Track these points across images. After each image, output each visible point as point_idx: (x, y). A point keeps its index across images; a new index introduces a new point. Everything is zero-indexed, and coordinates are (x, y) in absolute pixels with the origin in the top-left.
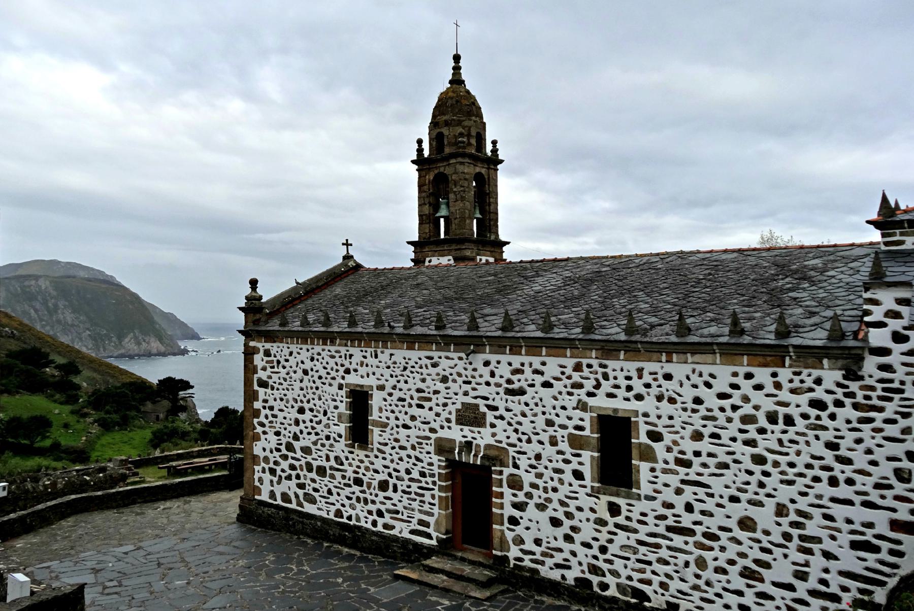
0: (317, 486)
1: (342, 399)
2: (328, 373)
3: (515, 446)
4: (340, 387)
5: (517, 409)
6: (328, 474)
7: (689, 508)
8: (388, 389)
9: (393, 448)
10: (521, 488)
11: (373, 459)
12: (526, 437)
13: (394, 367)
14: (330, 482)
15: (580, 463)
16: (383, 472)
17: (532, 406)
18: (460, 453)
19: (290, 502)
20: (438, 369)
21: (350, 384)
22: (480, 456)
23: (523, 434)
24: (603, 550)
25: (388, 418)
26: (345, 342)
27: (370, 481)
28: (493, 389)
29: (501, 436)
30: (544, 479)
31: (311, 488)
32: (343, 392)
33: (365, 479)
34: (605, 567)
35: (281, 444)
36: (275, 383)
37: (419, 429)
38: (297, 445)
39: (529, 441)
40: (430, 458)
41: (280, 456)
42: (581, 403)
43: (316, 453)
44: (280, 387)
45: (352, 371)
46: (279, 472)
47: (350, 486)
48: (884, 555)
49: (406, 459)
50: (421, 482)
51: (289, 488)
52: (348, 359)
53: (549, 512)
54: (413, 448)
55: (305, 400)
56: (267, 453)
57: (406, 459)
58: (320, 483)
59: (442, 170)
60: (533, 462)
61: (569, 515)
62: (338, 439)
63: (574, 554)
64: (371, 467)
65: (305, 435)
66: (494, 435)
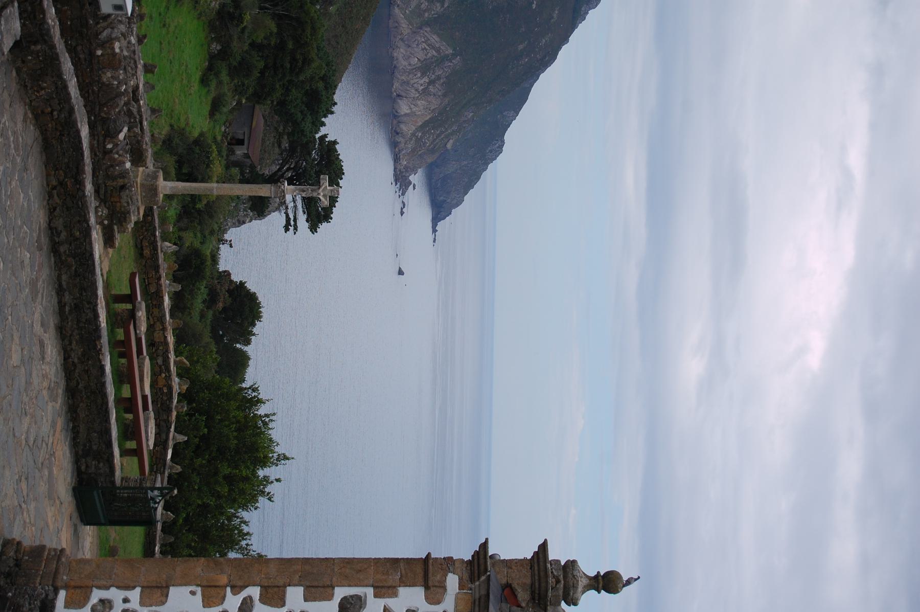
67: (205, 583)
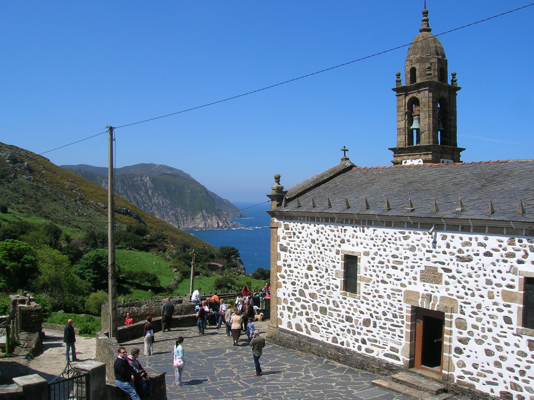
0: (320, 320)
1: (338, 261)
2: (329, 243)
3: (463, 298)
4: (338, 253)
5: (465, 271)
6: (328, 313)
8: (372, 255)
9: (374, 297)
10: (465, 328)
11: (359, 303)
12: (471, 292)
13: (376, 239)
14: (330, 318)
15: (510, 312)
16: (367, 313)
17: (476, 269)
18: (422, 303)
19: (302, 330)
20: (409, 241)
21: (345, 251)
22: (436, 305)
23: (469, 289)
24: (522, 373)
25: (371, 275)
26: (341, 220)
27: (357, 319)
28: (448, 256)
29: (453, 291)
30: (483, 322)
31: (316, 322)
32: (339, 256)
33: (354, 318)
34: (523, 385)
35: (296, 291)
36: (292, 248)
37: (393, 284)
38: (307, 292)
39: (473, 295)
40: (401, 305)
41: (295, 299)
42: (512, 269)
43: (320, 298)
44: (295, 251)
45: (346, 241)
46: (294, 310)
47: (343, 321)
49: (383, 305)
50: (393, 321)
51: (301, 321)
52: (343, 233)
53: (485, 346)
54: (389, 297)
55: (312, 261)
56: (286, 296)
57: (383, 305)
58: (322, 319)
59: (415, 95)
60: (475, 310)
61: (499, 348)
62: (335, 289)
63: (501, 375)
64: (359, 309)
65: (312, 285)
66: (447, 290)
67: (276, 288)
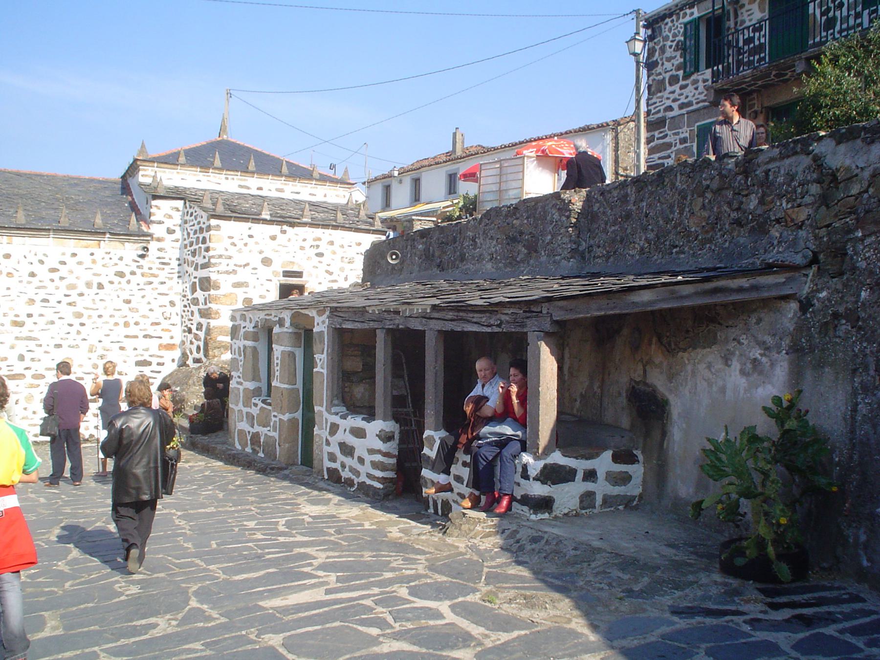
7: (21, 358)
48: (154, 367)
